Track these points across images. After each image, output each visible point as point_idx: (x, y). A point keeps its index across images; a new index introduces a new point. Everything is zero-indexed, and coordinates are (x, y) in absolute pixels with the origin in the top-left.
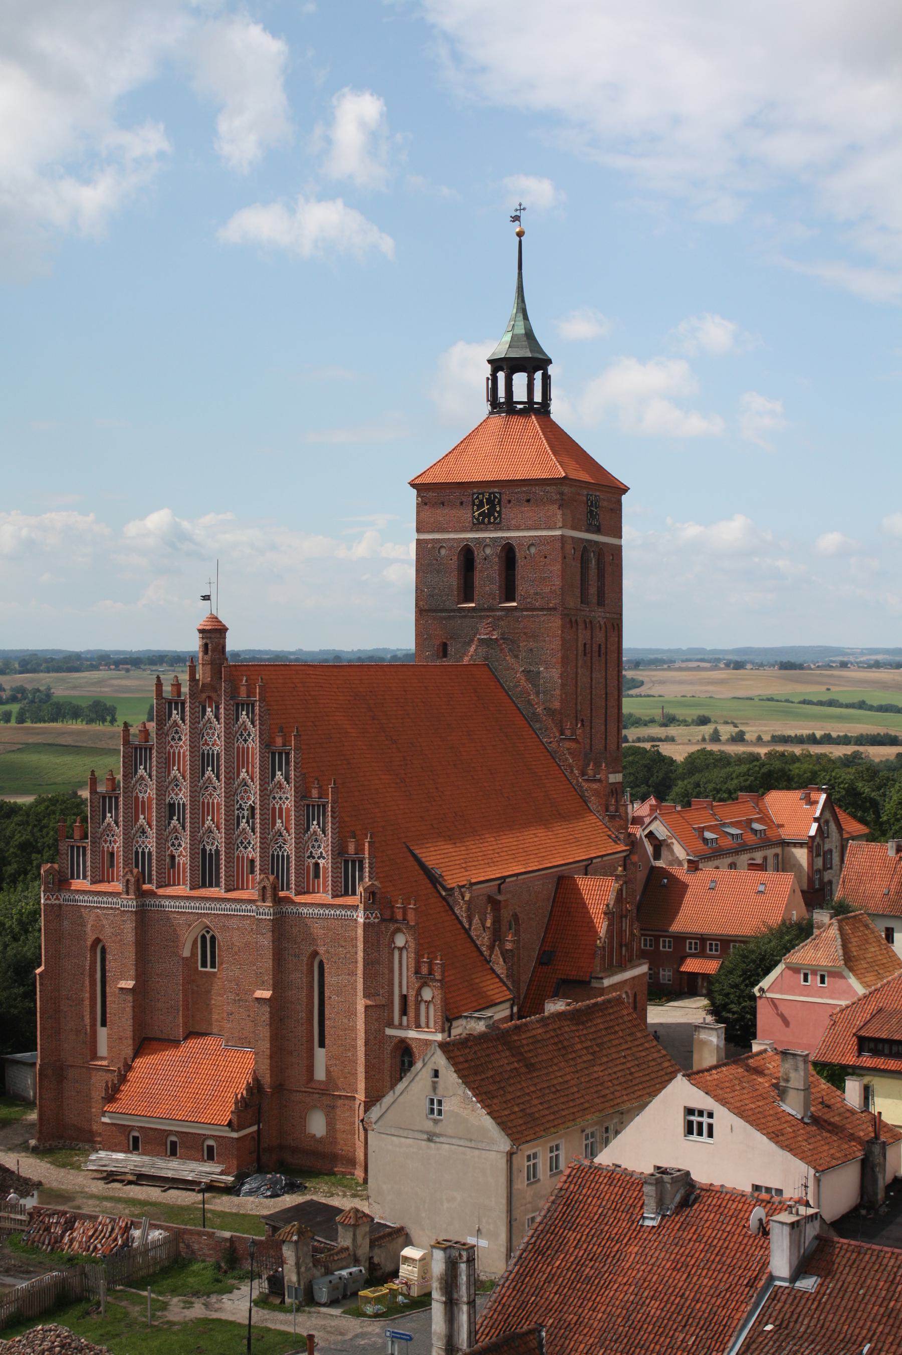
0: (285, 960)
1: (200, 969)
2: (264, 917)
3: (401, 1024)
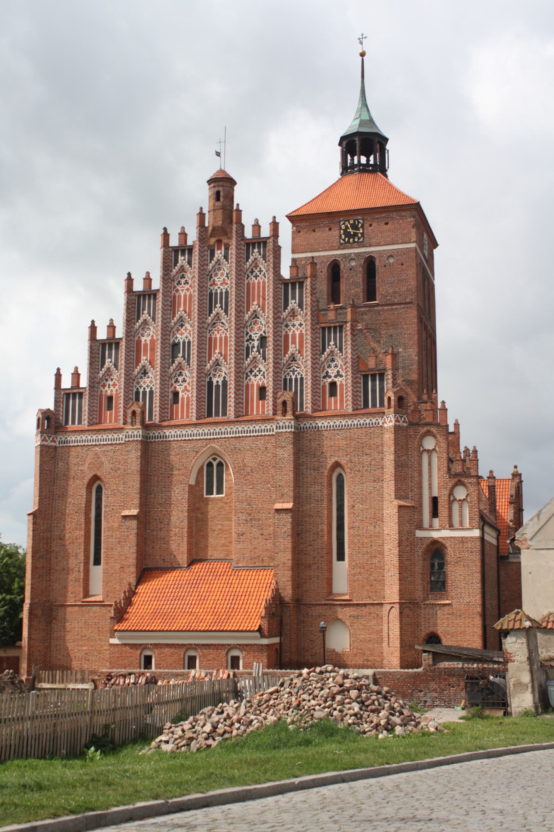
0: (303, 474)
1: (205, 496)
2: (284, 430)
3: (431, 526)
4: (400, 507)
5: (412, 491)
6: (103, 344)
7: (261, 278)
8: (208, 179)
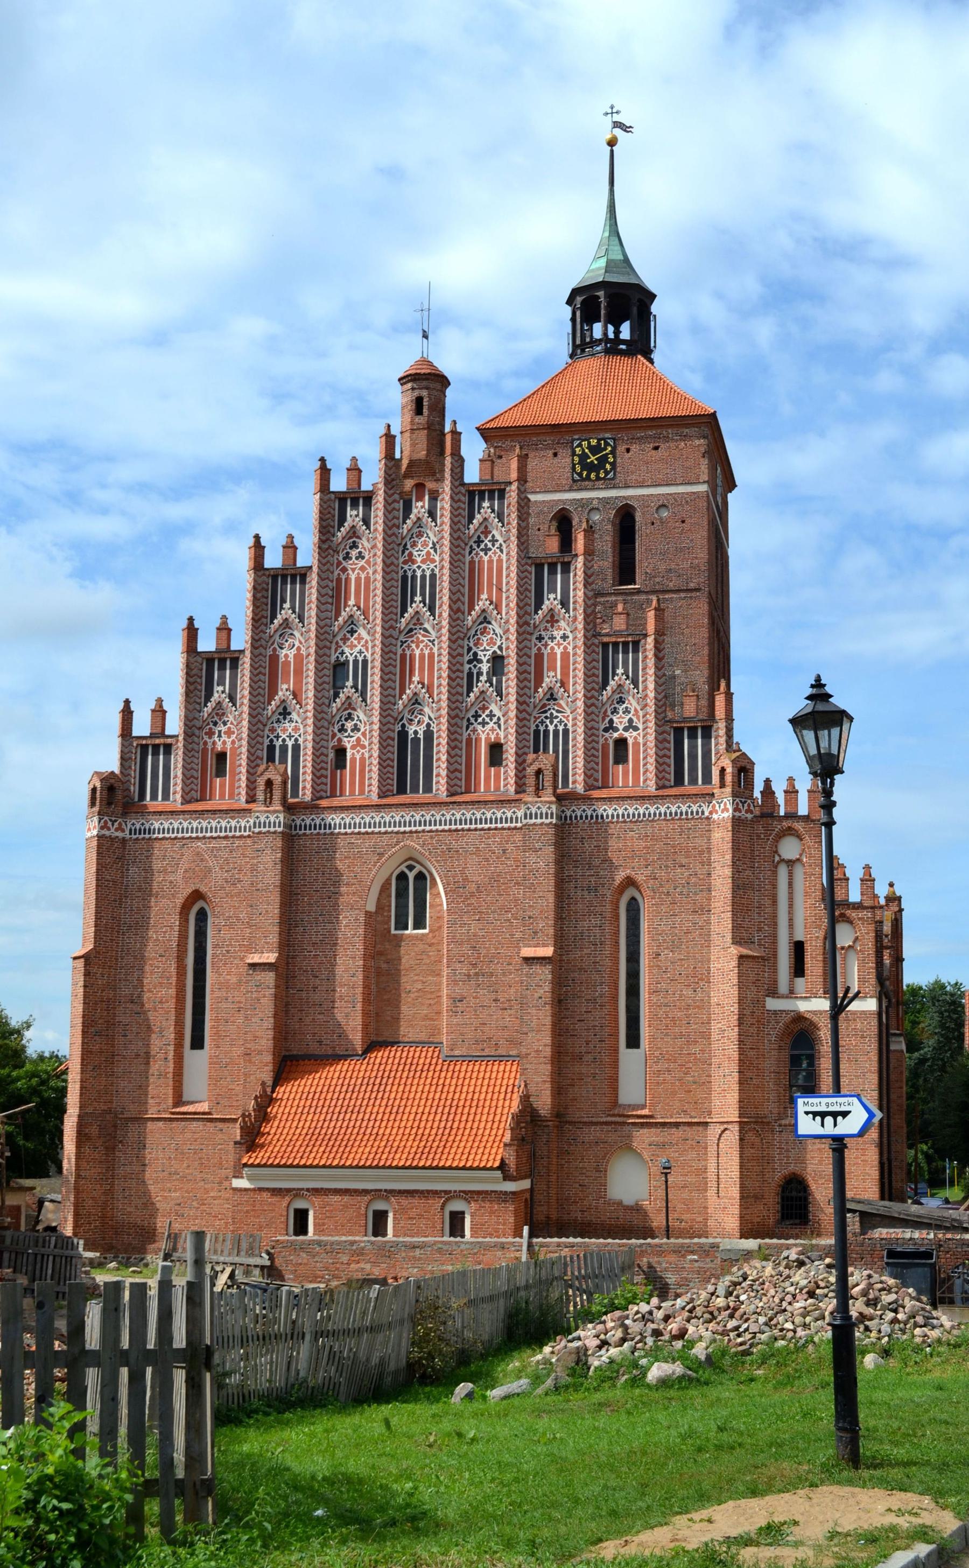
0: (569, 897)
1: (393, 932)
2: (539, 821)
3: (792, 991)
4: (741, 957)
5: (759, 930)
6: (209, 659)
7: (495, 553)
8: (401, 374)
